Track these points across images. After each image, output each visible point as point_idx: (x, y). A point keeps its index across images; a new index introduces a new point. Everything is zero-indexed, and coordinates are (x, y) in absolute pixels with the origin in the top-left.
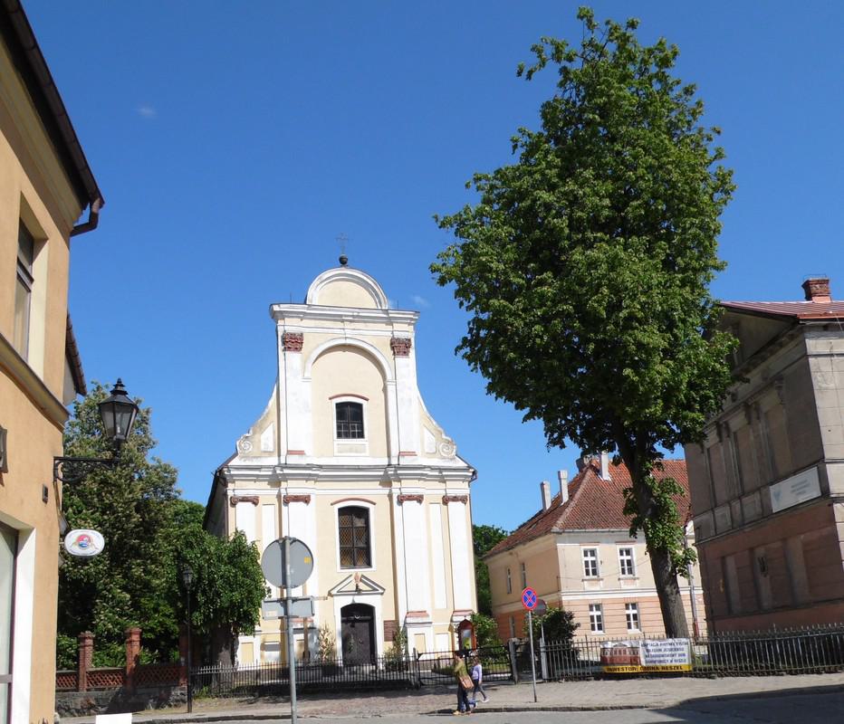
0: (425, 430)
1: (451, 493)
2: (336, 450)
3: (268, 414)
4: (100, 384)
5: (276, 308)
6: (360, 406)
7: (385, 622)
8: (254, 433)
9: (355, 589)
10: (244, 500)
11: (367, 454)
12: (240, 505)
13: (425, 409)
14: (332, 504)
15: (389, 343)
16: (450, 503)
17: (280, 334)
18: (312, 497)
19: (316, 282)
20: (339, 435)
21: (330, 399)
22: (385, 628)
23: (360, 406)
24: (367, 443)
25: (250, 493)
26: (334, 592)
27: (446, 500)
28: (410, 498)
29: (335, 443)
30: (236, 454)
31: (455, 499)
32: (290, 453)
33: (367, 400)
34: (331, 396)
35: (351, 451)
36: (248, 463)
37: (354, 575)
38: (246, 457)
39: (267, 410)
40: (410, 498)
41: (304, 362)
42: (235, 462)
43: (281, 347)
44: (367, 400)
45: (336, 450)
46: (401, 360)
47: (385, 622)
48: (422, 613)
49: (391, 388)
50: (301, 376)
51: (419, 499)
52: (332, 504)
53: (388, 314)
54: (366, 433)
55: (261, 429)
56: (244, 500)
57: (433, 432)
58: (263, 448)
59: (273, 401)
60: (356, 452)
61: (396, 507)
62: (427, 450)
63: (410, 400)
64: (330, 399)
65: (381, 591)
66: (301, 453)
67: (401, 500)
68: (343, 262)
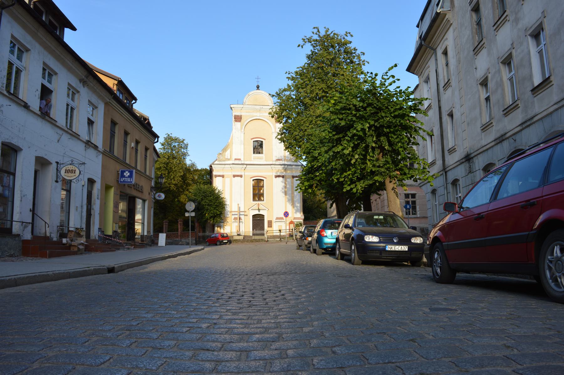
2: (252, 159)
4: (169, 134)
5: (232, 106)
6: (262, 142)
8: (223, 152)
10: (219, 176)
11: (264, 160)
12: (218, 178)
18: (243, 176)
19: (247, 96)
20: (254, 153)
22: (268, 223)
23: (262, 142)
25: (221, 174)
26: (250, 209)
29: (252, 156)
30: (216, 160)
32: (236, 159)
33: (265, 139)
34: (252, 138)
35: (258, 159)
36: (221, 163)
38: (220, 161)
41: (241, 126)
42: (216, 162)
43: (233, 119)
44: (265, 139)
45: (252, 159)
50: (240, 131)
54: (264, 152)
55: (226, 150)
56: (219, 176)
58: (226, 157)
60: (260, 159)
64: (251, 139)
65: (267, 209)
66: (239, 159)
68: (258, 87)
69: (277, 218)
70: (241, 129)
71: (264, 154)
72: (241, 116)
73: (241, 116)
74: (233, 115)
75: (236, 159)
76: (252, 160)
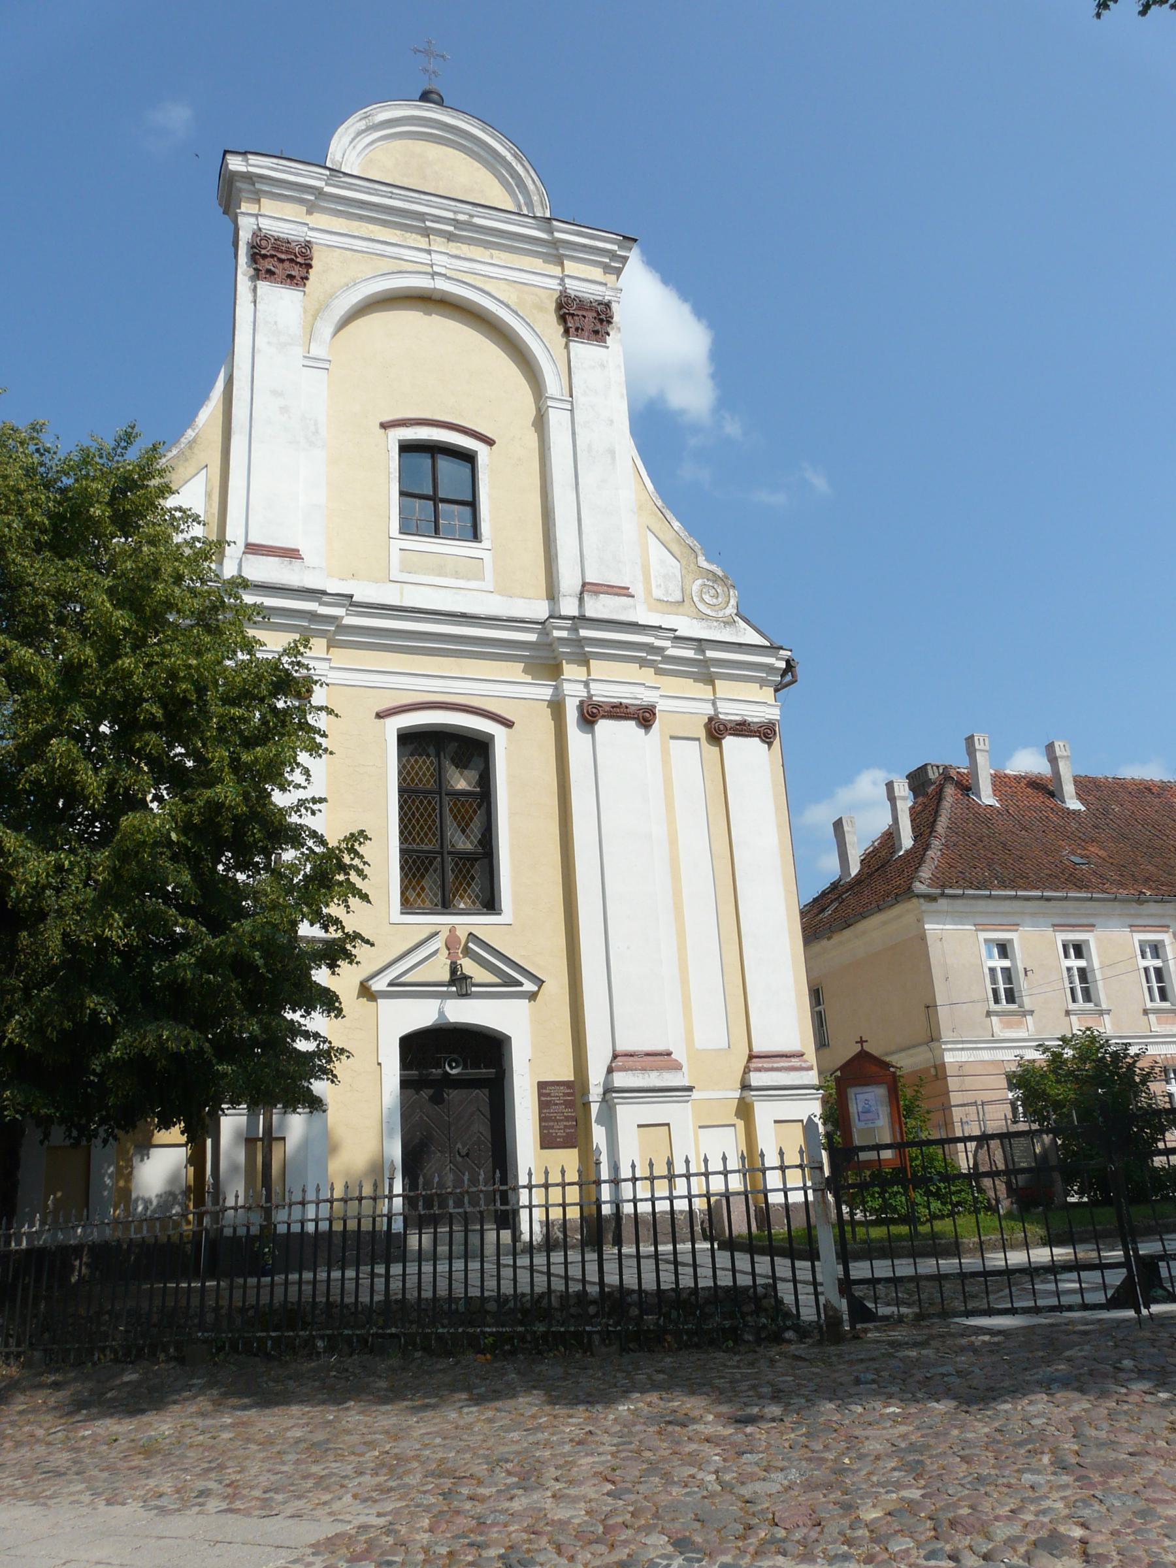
0: (651, 539)
1: (730, 712)
3: (191, 444)
5: (236, 164)
7: (542, 1085)
9: (446, 976)
11: (488, 584)
13: (650, 487)
14: (379, 716)
15: (553, 306)
16: (729, 742)
17: (245, 236)
21: (384, 426)
24: (486, 555)
27: (716, 731)
28: (618, 712)
31: (742, 729)
32: (252, 549)
33: (490, 442)
34: (387, 418)
37: (444, 934)
39: (190, 434)
40: (618, 712)
44: (490, 442)
46: (582, 351)
47: (542, 1085)
48: (661, 1059)
49: (557, 419)
50: (299, 351)
51: (645, 717)
52: (379, 716)
53: (551, 231)
54: (485, 528)
57: (675, 548)
59: (209, 413)
60: (457, 575)
61: (576, 737)
62: (658, 593)
63: (612, 453)
67: (590, 715)
69: (619, 1059)
70: (310, 334)
71: (486, 543)
72: (308, 245)
73: (308, 245)
74: (245, 236)
75: (252, 549)
76: (395, 574)
